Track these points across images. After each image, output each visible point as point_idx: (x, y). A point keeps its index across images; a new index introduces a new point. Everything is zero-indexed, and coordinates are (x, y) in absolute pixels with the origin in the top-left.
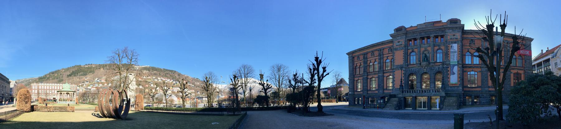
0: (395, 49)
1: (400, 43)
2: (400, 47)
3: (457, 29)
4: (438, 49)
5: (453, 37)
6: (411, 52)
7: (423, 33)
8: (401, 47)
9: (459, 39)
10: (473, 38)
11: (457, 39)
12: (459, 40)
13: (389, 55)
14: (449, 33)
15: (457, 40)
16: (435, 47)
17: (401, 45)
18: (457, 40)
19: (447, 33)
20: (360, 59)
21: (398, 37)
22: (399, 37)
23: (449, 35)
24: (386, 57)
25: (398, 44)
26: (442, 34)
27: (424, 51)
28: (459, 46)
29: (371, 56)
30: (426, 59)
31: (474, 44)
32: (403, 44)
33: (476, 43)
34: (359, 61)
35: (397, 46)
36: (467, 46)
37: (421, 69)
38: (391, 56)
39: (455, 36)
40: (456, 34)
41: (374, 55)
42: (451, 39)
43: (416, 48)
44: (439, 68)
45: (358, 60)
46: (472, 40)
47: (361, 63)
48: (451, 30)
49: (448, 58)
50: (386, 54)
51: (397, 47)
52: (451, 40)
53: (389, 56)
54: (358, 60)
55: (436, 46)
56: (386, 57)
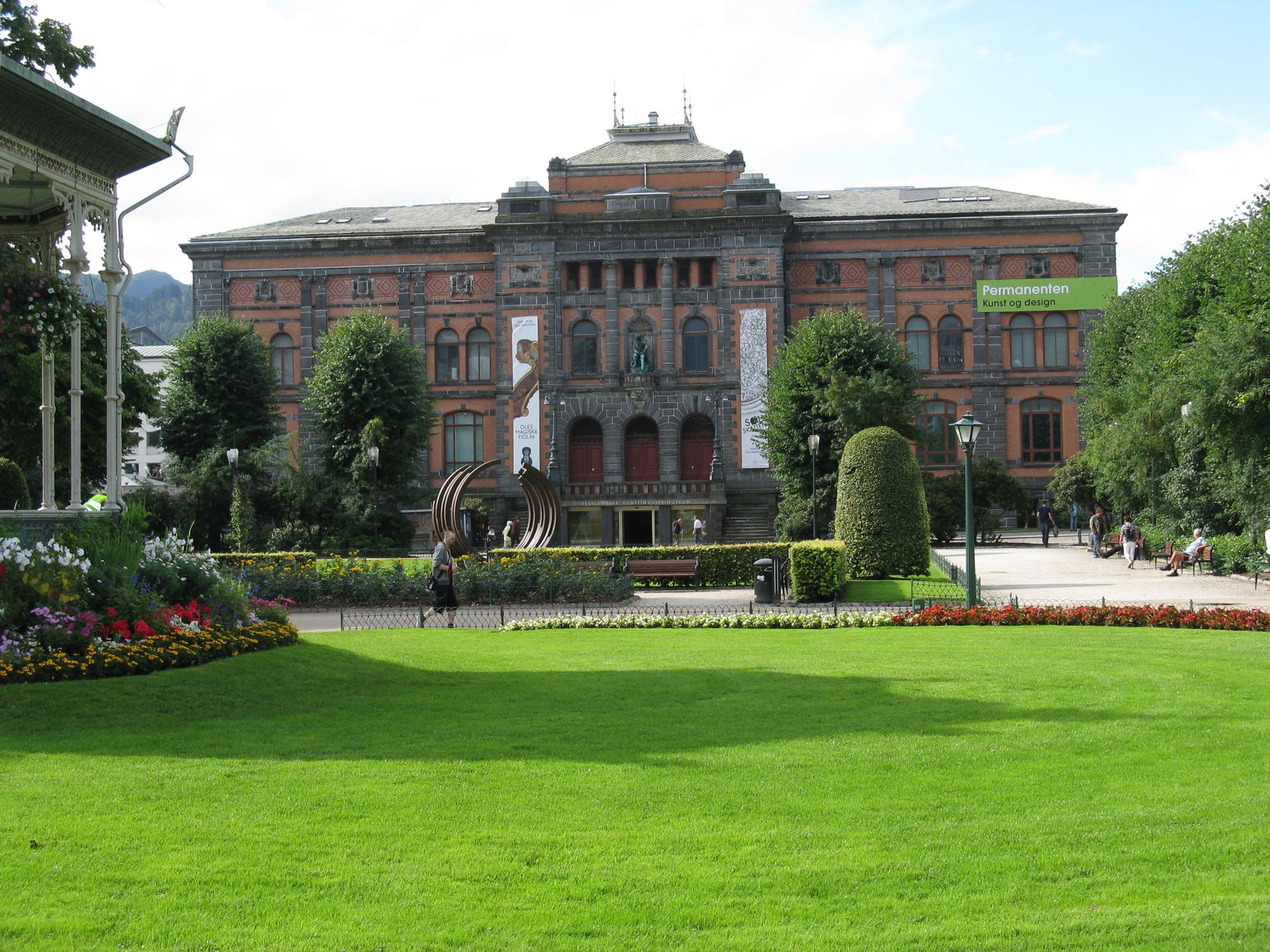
0: (507, 302)
1: (530, 276)
2: (528, 294)
3: (765, 233)
4: (689, 319)
5: (747, 270)
6: (578, 322)
7: (629, 243)
8: (535, 294)
9: (772, 279)
10: (829, 256)
11: (764, 278)
12: (775, 282)
13: (457, 309)
14: (733, 252)
15: (765, 283)
16: (678, 308)
17: (536, 285)
18: (765, 283)
19: (724, 251)
20: (280, 303)
21: (520, 241)
22: (527, 247)
23: (730, 261)
24: (437, 316)
25: (519, 276)
26: (707, 254)
27: (634, 322)
28: (775, 311)
29: (355, 296)
30: (642, 361)
31: (838, 281)
32: (544, 280)
33: (843, 277)
34: (270, 308)
35: (513, 285)
36: (805, 292)
37: (624, 400)
38: (470, 315)
39: (757, 268)
40: (758, 258)
41: (371, 296)
42: (742, 278)
43: (598, 307)
44: (696, 400)
45: (261, 304)
46: (827, 264)
47: (281, 326)
48: (742, 238)
49: (733, 360)
50: (441, 303)
51: (514, 290)
52: (741, 284)
53: (454, 315)
54: (261, 304)
55: (682, 304)
56: (437, 316)
